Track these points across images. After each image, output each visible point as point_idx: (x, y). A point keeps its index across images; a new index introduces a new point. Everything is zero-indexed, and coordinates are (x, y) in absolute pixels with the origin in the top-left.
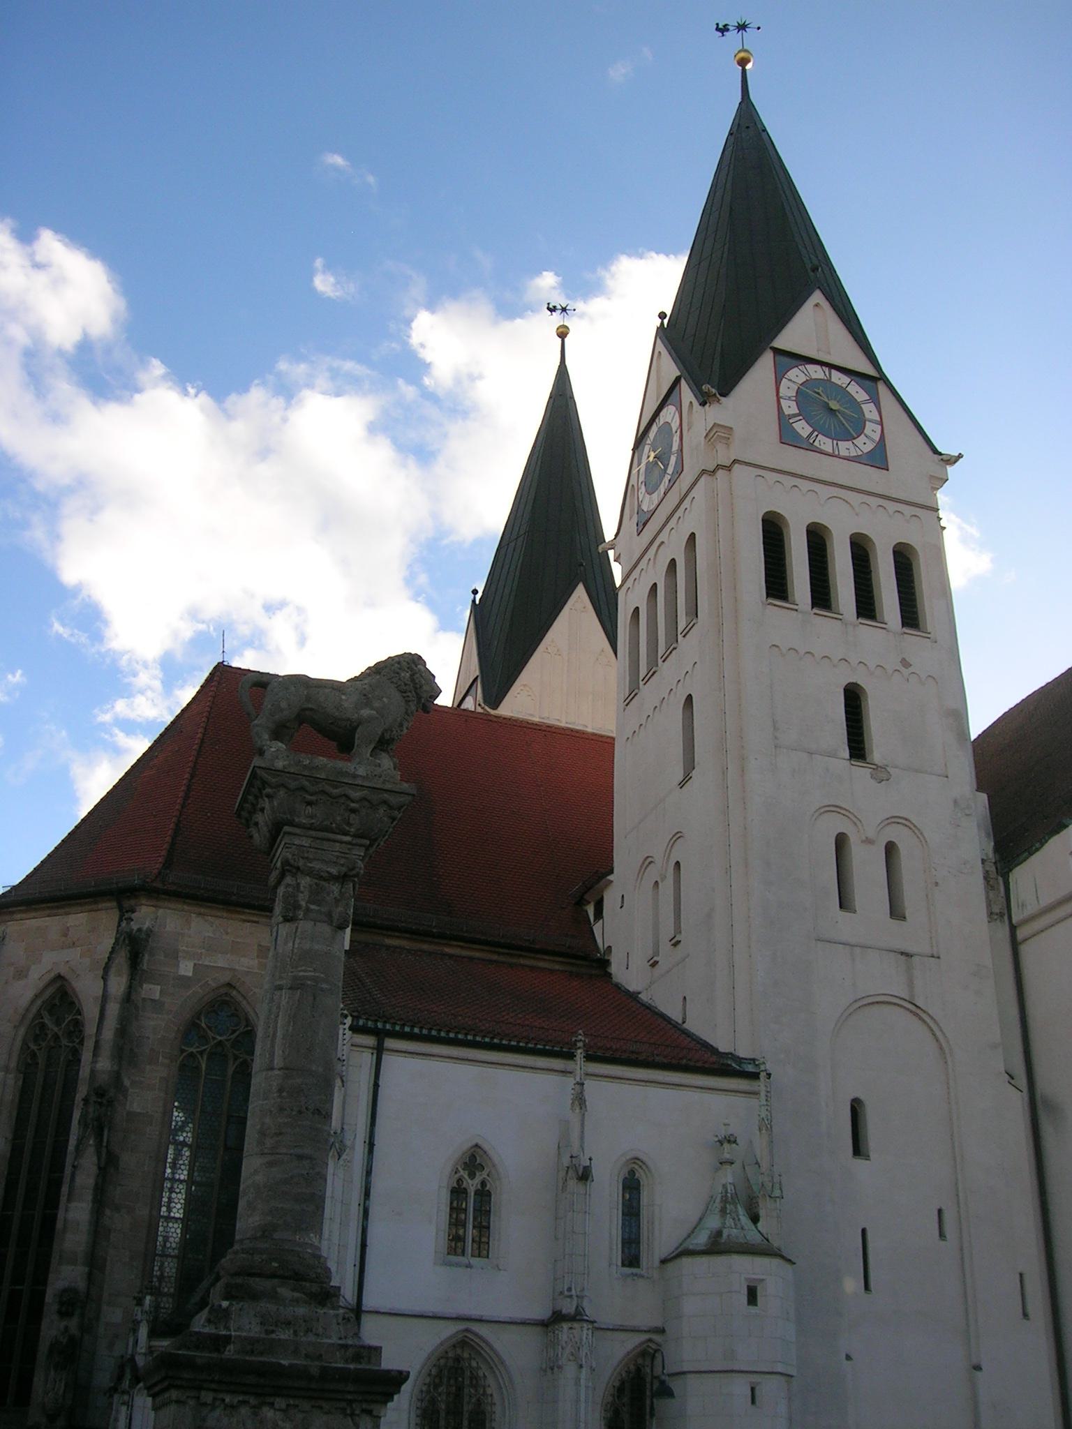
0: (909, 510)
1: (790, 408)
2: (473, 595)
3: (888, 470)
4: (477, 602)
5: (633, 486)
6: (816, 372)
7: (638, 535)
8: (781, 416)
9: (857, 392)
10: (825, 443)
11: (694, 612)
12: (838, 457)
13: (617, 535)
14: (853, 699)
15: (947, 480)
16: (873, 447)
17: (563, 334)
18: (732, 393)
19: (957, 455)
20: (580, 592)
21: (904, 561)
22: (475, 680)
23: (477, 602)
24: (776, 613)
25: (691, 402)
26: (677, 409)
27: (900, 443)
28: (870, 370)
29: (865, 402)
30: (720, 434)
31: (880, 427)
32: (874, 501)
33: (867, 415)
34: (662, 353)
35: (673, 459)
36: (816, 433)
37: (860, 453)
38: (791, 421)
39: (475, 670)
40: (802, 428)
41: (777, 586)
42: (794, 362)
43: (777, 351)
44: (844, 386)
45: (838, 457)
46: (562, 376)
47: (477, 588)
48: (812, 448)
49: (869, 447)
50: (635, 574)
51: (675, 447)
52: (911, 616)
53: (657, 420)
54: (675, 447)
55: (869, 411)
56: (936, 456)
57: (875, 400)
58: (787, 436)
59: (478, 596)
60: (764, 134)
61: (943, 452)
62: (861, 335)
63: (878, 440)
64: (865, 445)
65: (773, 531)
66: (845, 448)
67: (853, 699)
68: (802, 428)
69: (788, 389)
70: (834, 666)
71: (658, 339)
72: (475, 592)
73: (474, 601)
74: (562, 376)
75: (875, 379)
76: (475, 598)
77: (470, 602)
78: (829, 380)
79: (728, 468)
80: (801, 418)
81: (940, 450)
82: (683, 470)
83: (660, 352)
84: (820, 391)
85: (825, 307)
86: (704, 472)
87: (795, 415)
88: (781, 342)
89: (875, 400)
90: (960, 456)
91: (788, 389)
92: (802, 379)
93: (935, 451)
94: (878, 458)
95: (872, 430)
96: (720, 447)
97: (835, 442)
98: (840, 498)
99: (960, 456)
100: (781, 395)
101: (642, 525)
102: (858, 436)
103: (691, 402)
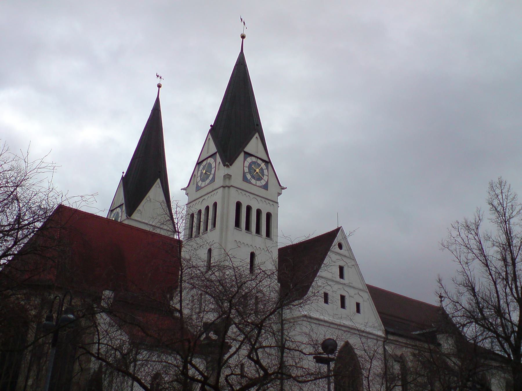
0: (271, 203)
1: (246, 170)
2: (122, 174)
3: (268, 190)
4: (124, 176)
5: (195, 175)
6: (254, 159)
7: (196, 192)
9: (263, 165)
10: (253, 181)
11: (214, 225)
12: (256, 186)
13: (187, 187)
14: (253, 255)
15: (281, 194)
17: (159, 86)
18: (233, 165)
19: (285, 187)
20: (159, 180)
21: (269, 215)
22: (123, 204)
23: (124, 176)
24: (237, 232)
25: (220, 162)
26: (214, 161)
27: (272, 182)
28: (267, 160)
30: (228, 177)
31: (267, 177)
32: (263, 200)
34: (210, 139)
35: (211, 176)
36: (252, 178)
37: (262, 185)
39: (122, 199)
40: (249, 176)
41: (237, 224)
43: (246, 153)
44: (260, 164)
45: (256, 186)
46: (158, 101)
47: (124, 172)
48: (250, 183)
50: (194, 203)
51: (213, 172)
52: (268, 234)
53: (207, 160)
54: (213, 172)
55: (265, 172)
56: (280, 187)
57: (267, 168)
58: (245, 179)
59: (124, 174)
60: (246, 67)
61: (282, 186)
62: (264, 143)
63: (266, 181)
64: (263, 182)
65: (239, 205)
66: (259, 183)
67: (253, 255)
68: (249, 176)
69: (247, 164)
70: (249, 247)
71: (209, 134)
72: (123, 173)
73: (123, 176)
74: (158, 101)
75: (268, 162)
76: (123, 175)
77: (122, 176)
79: (229, 187)
80: (249, 173)
81: (281, 185)
82: (214, 181)
83: (209, 139)
85: (259, 139)
86: (222, 186)
87: (247, 172)
88: (247, 149)
89: (267, 168)
90: (286, 188)
92: (250, 161)
93: (280, 185)
94: (266, 187)
95: (265, 178)
96: (227, 180)
98: (256, 199)
99: (286, 188)
100: (245, 166)
101: (198, 188)
103: (220, 162)
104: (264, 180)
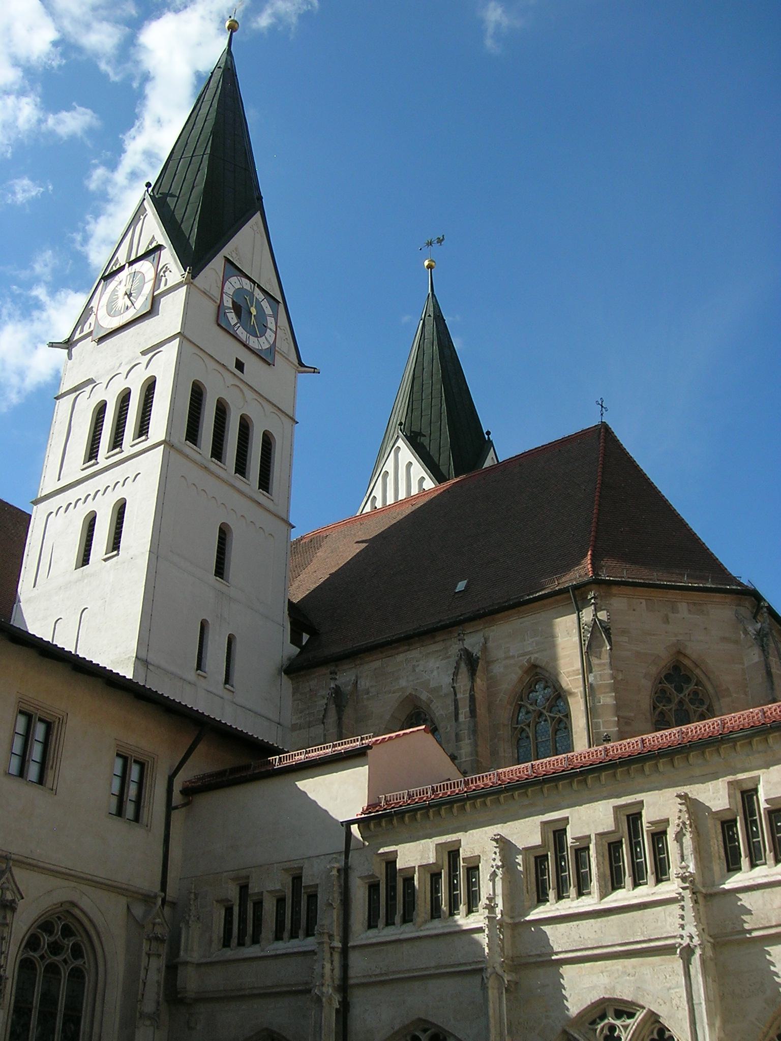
1: (228, 303)
6: (247, 284)
8: (220, 307)
16: (268, 347)
29: (270, 316)
33: (269, 325)
36: (239, 325)
38: (227, 311)
42: (238, 273)
49: (266, 346)
55: (271, 322)
57: (275, 316)
69: (229, 289)
75: (278, 301)
78: (252, 293)
84: (247, 298)
87: (229, 308)
89: (275, 316)
90: (315, 371)
91: (229, 289)
92: (238, 286)
97: (248, 335)
99: (315, 371)
102: (261, 337)
104: (266, 338)
